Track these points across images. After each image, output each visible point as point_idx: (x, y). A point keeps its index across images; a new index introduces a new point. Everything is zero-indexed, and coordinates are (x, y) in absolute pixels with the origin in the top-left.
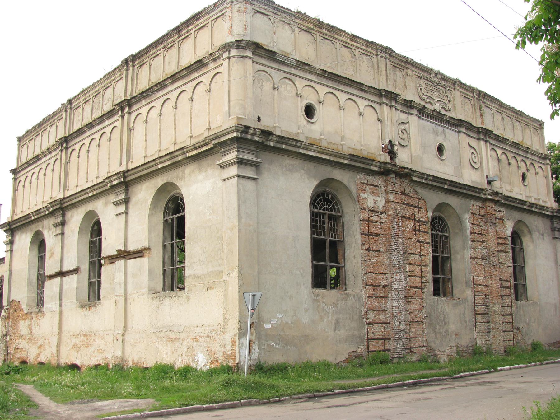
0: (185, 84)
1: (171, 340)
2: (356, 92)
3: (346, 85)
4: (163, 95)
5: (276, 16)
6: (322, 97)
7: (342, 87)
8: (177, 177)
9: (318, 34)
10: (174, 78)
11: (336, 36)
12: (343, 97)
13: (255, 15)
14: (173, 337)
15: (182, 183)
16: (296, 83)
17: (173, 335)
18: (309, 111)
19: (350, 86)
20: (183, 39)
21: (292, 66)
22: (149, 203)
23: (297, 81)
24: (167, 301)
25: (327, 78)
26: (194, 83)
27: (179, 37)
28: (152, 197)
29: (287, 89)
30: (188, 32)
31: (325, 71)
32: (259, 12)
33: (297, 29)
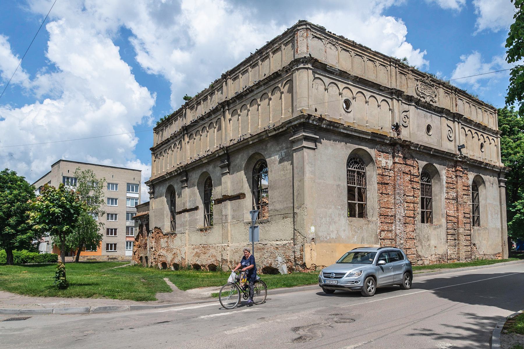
0: (266, 89)
9: (353, 52)
11: (365, 53)
12: (368, 94)
16: (339, 86)
18: (347, 103)
23: (339, 84)
25: (358, 82)
26: (273, 88)
29: (333, 89)
31: (358, 77)
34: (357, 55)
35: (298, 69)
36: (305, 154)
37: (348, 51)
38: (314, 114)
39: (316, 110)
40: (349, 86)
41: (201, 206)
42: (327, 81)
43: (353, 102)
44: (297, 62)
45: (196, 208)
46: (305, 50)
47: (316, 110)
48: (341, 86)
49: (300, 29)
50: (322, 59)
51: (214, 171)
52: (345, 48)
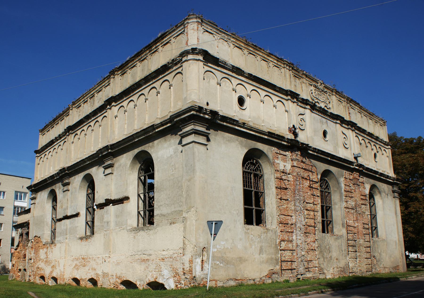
1: (144, 260)
5: (217, 34)
7: (262, 87)
8: (149, 147)
9: (246, 50)
13: (204, 33)
14: (146, 258)
15: (152, 150)
16: (232, 81)
17: (146, 257)
18: (241, 101)
21: (229, 70)
22: (128, 166)
23: (233, 80)
24: (142, 233)
28: (130, 162)
31: (251, 75)
32: (207, 31)
34: (250, 53)
35: (186, 61)
36: (196, 150)
37: (241, 49)
38: (205, 107)
39: (208, 104)
41: (83, 212)
42: (220, 75)
43: (247, 99)
44: (185, 53)
45: (77, 215)
46: (195, 42)
47: (208, 104)
48: (235, 82)
49: (191, 22)
50: (213, 52)
51: (97, 172)
52: (238, 46)
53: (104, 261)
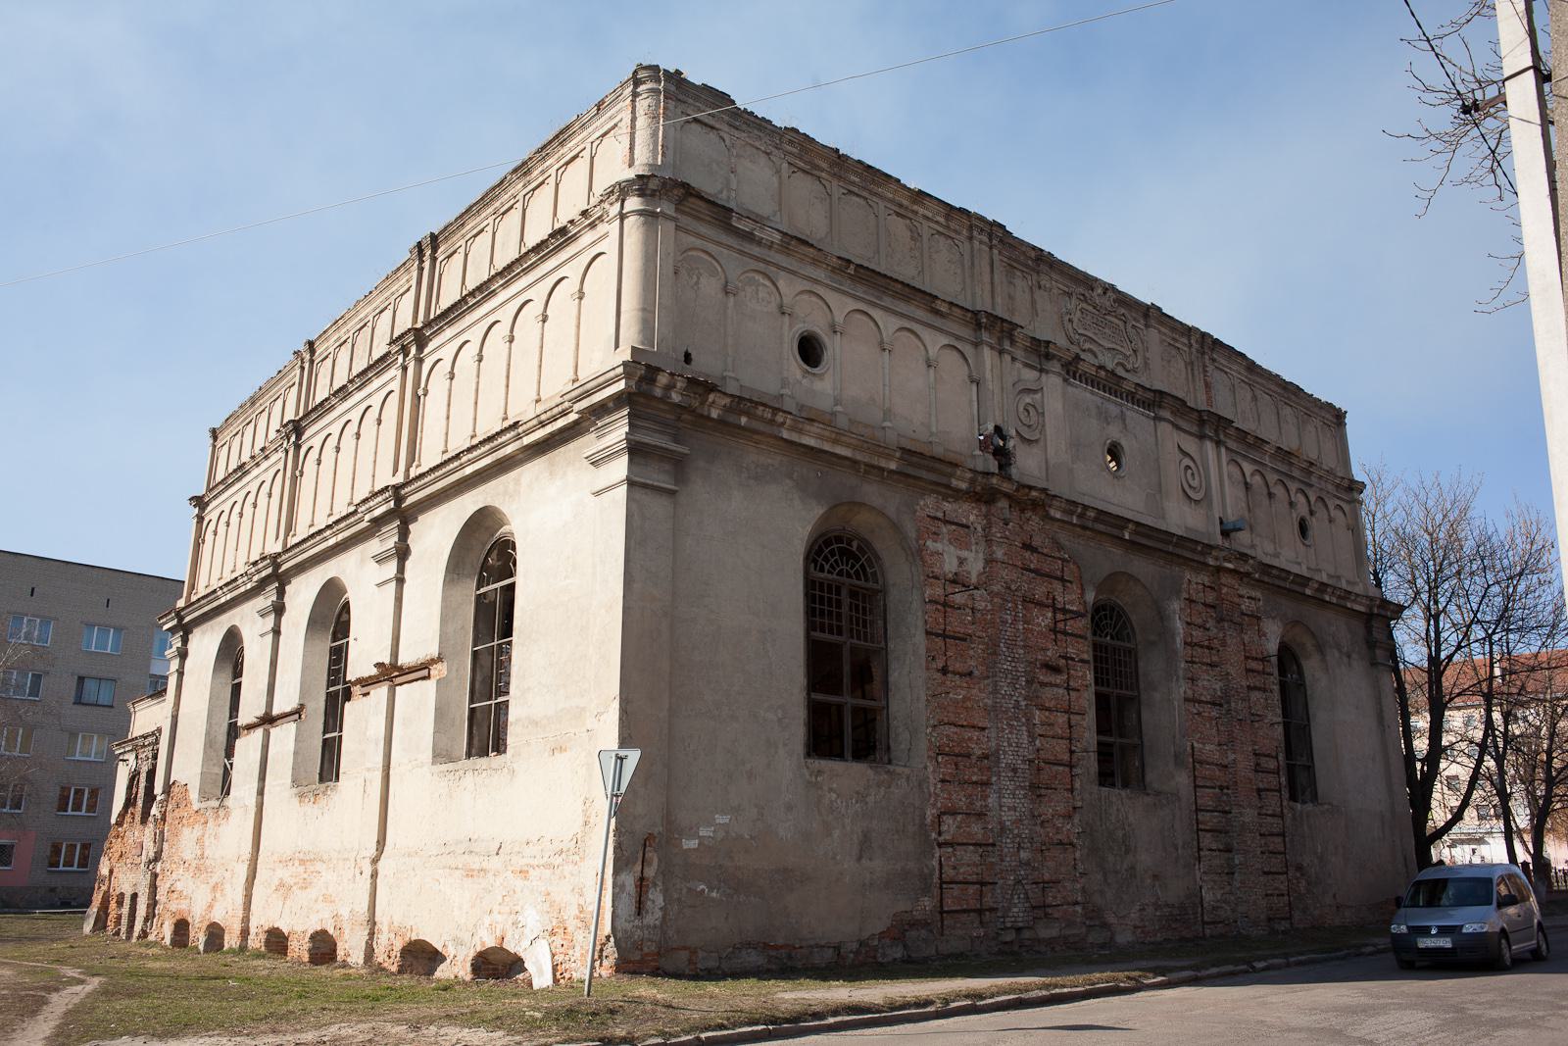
0: (530, 286)
2: (920, 314)
3: (896, 295)
4: (487, 315)
6: (839, 318)
7: (887, 301)
9: (835, 183)
10: (508, 273)
12: (889, 324)
18: (810, 350)
19: (907, 299)
20: (534, 190)
27: (525, 186)
30: (543, 172)
31: (849, 262)
33: (785, 165)
40: (821, 290)
53: (358, 872)
